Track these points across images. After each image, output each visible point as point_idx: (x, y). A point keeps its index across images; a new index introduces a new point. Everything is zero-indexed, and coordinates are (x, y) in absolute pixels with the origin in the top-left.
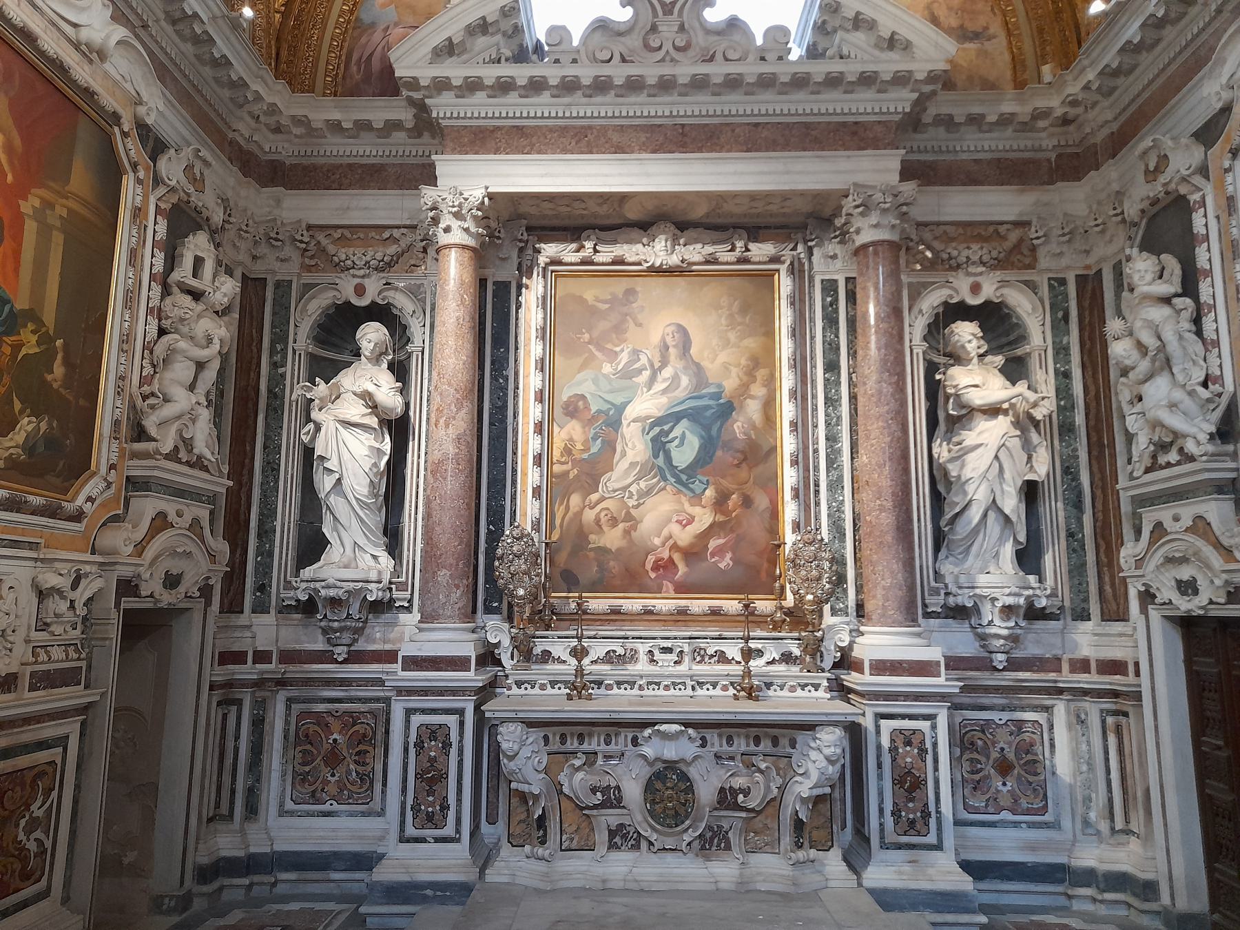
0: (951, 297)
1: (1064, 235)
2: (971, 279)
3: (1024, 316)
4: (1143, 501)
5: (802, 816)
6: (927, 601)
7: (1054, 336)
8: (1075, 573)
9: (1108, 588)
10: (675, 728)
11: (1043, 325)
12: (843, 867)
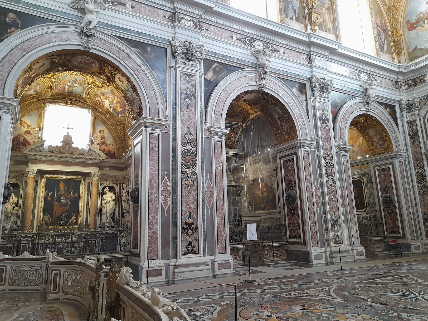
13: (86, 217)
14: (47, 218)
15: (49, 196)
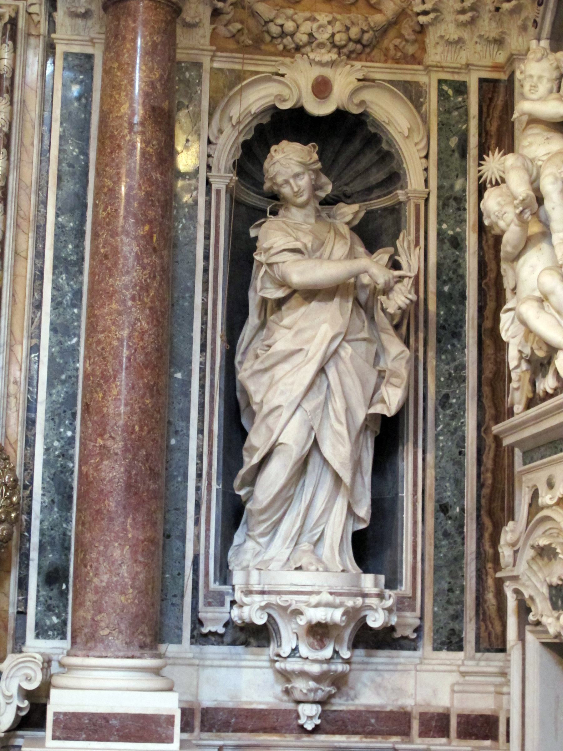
1: (463, 11)
2: (316, 72)
3: (398, 138)
6: (201, 615)
7: (442, 176)
8: (445, 572)
9: (490, 597)
11: (427, 157)
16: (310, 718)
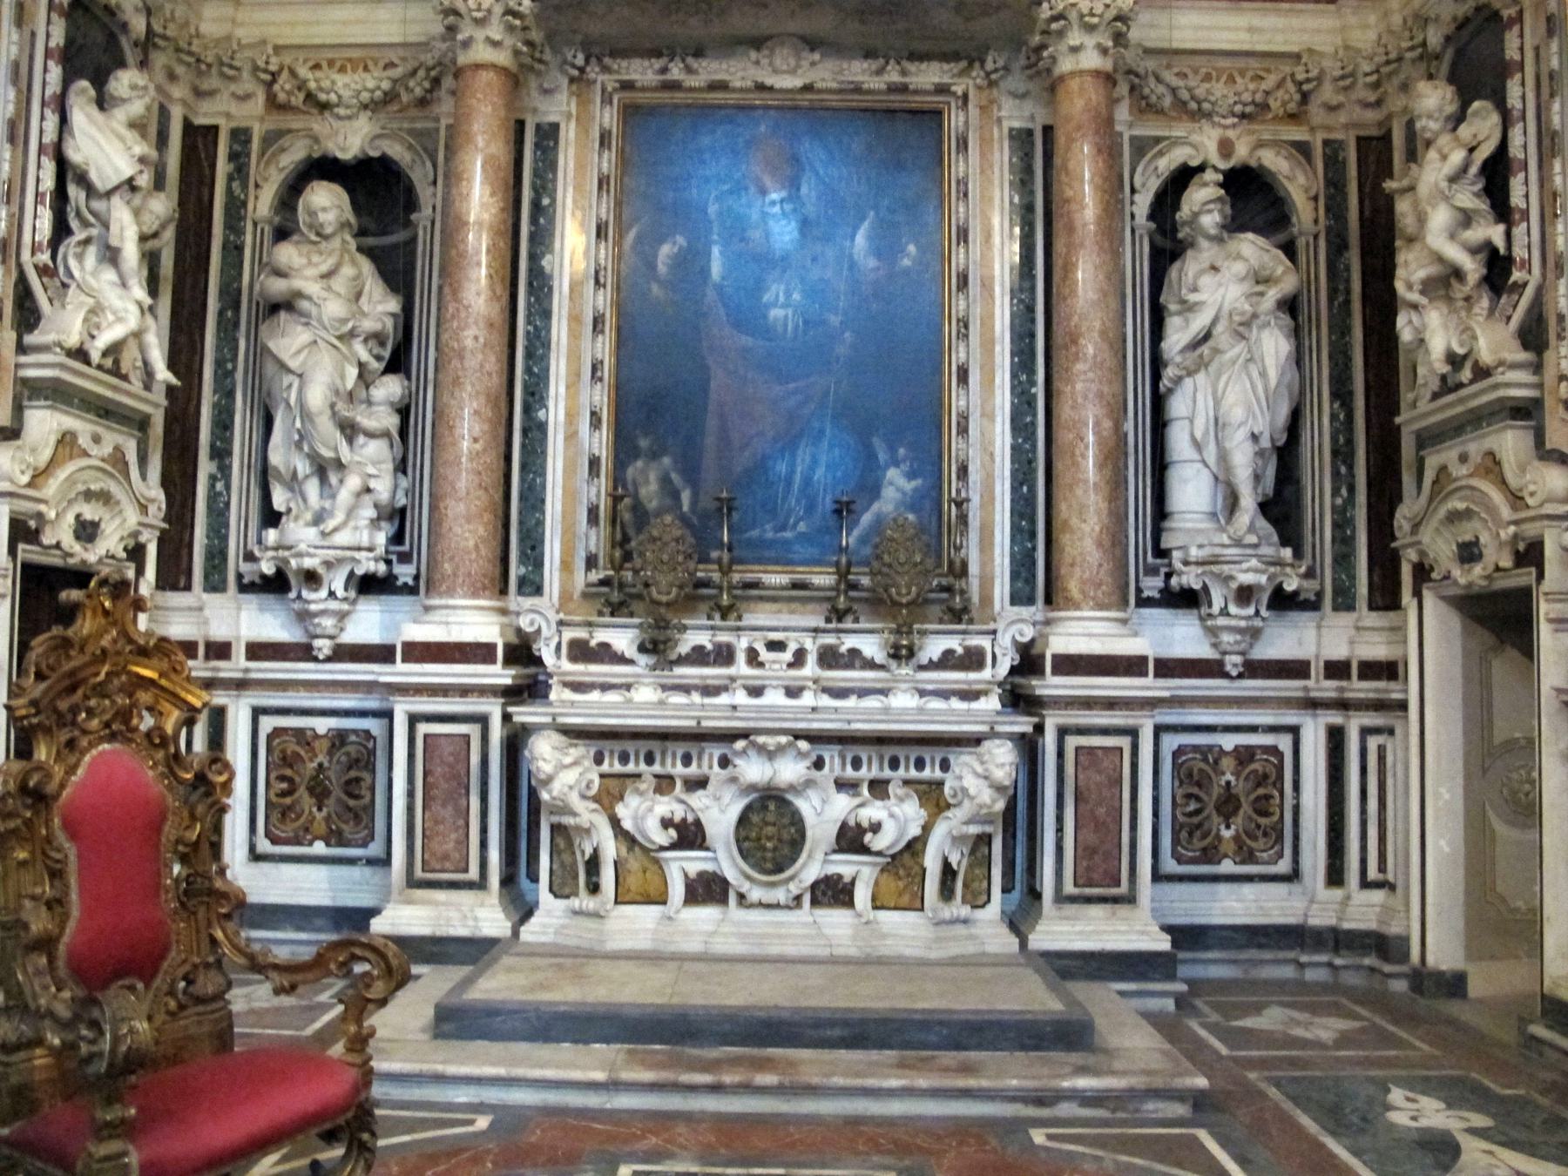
0: (1191, 157)
4: (1429, 439)
5: (954, 860)
6: (1142, 585)
10: (783, 739)
12: (1004, 930)
13: (1015, 489)
14: (653, 486)
15: (662, 268)
16: (1235, 665)
